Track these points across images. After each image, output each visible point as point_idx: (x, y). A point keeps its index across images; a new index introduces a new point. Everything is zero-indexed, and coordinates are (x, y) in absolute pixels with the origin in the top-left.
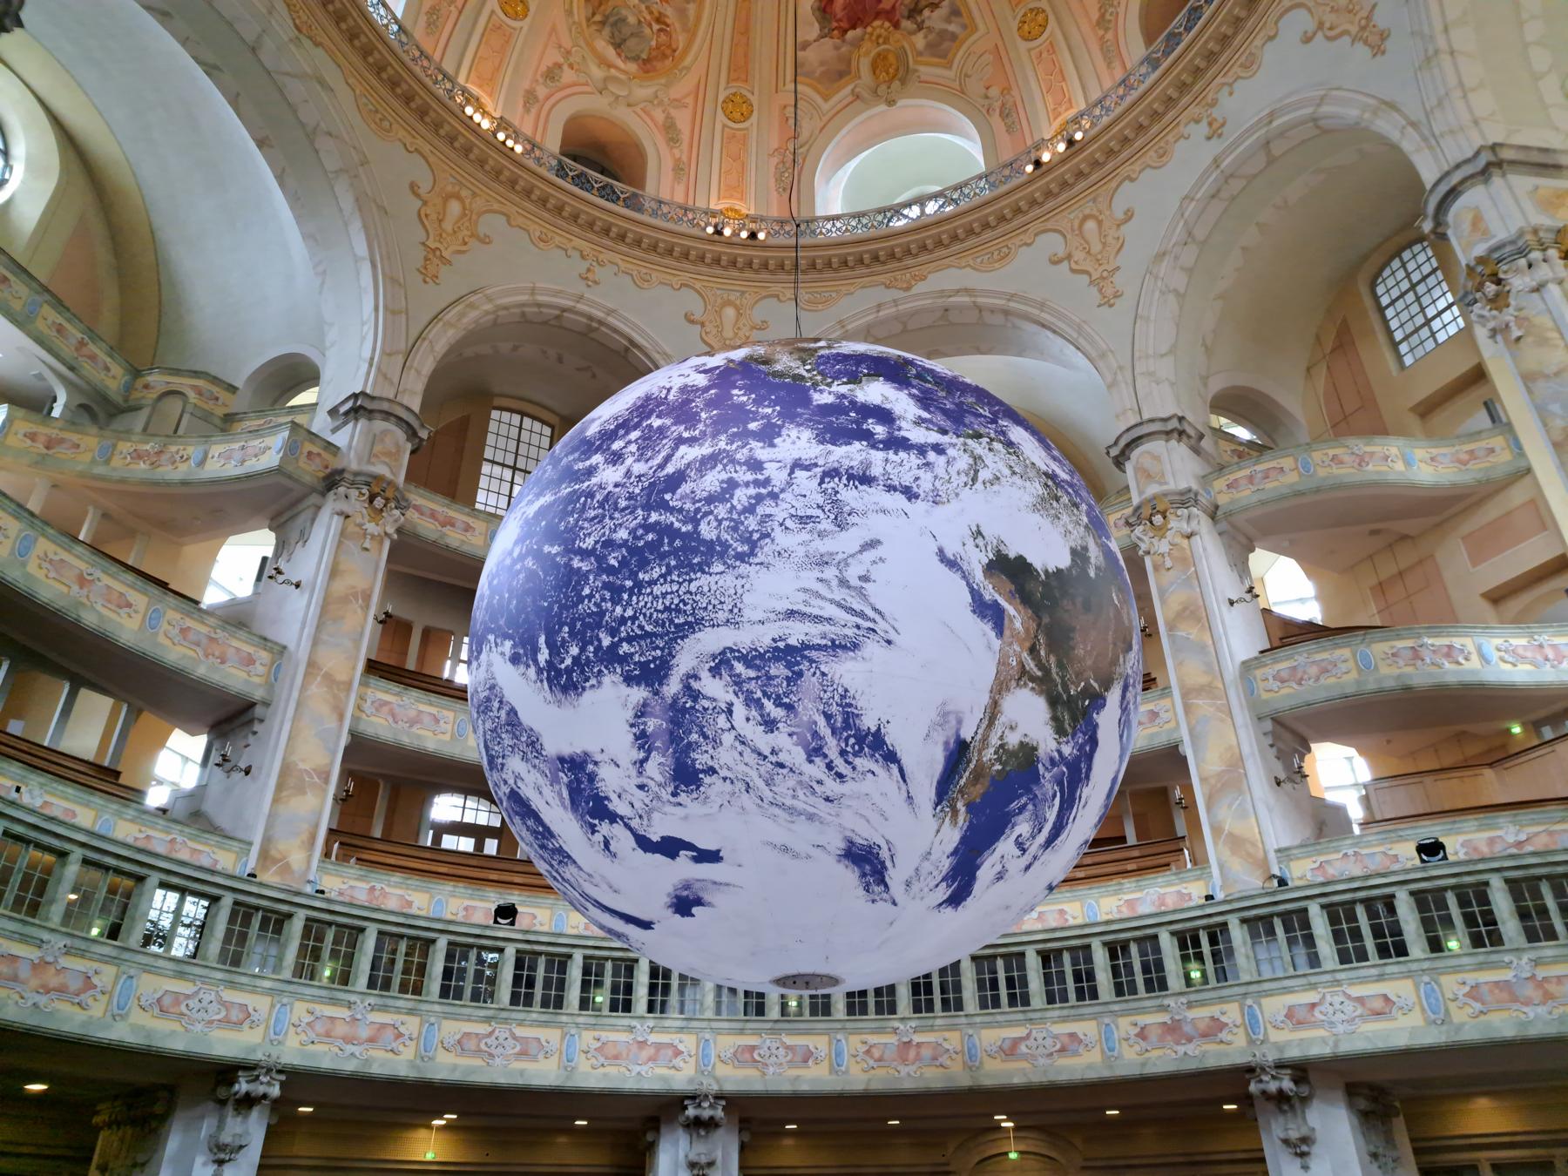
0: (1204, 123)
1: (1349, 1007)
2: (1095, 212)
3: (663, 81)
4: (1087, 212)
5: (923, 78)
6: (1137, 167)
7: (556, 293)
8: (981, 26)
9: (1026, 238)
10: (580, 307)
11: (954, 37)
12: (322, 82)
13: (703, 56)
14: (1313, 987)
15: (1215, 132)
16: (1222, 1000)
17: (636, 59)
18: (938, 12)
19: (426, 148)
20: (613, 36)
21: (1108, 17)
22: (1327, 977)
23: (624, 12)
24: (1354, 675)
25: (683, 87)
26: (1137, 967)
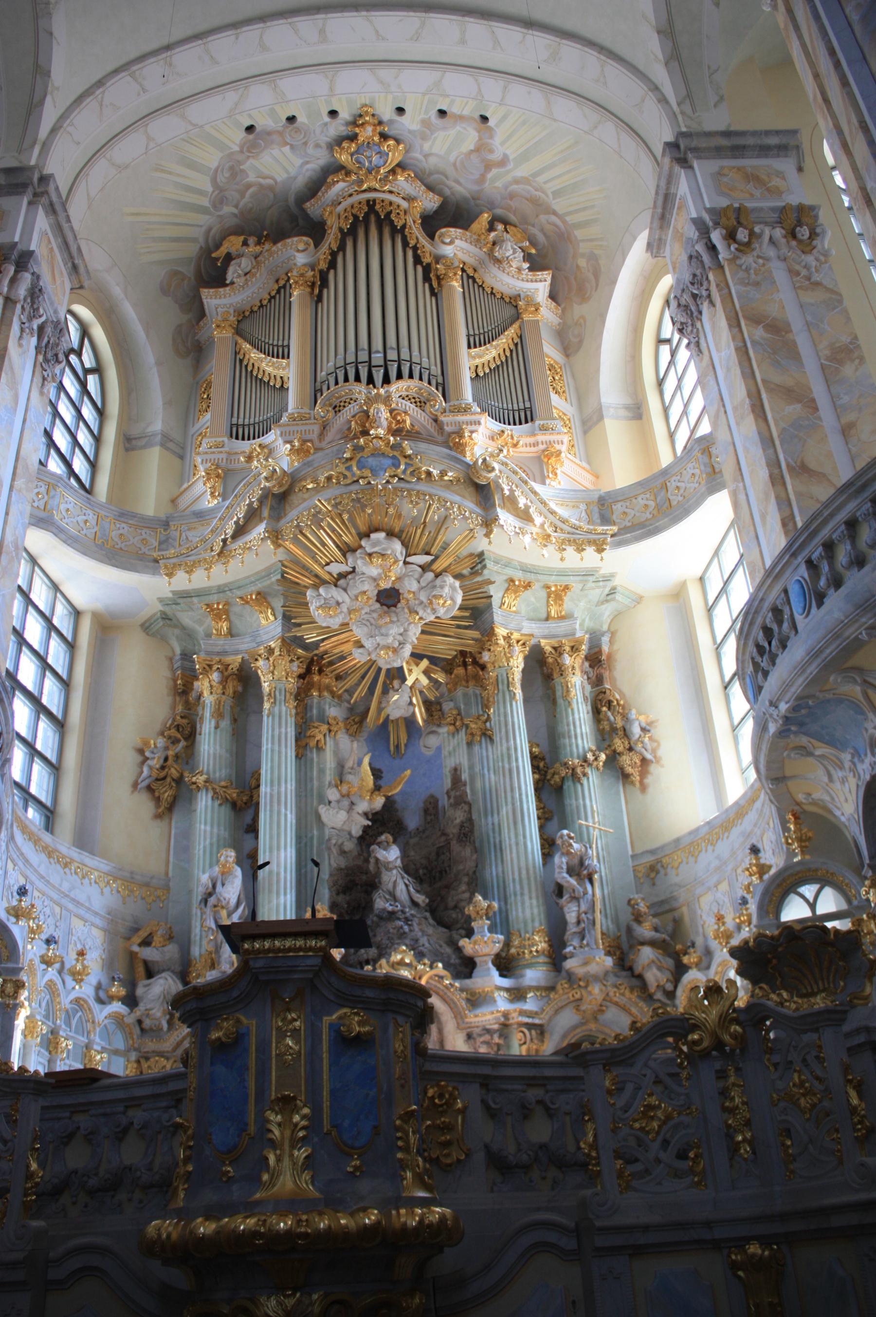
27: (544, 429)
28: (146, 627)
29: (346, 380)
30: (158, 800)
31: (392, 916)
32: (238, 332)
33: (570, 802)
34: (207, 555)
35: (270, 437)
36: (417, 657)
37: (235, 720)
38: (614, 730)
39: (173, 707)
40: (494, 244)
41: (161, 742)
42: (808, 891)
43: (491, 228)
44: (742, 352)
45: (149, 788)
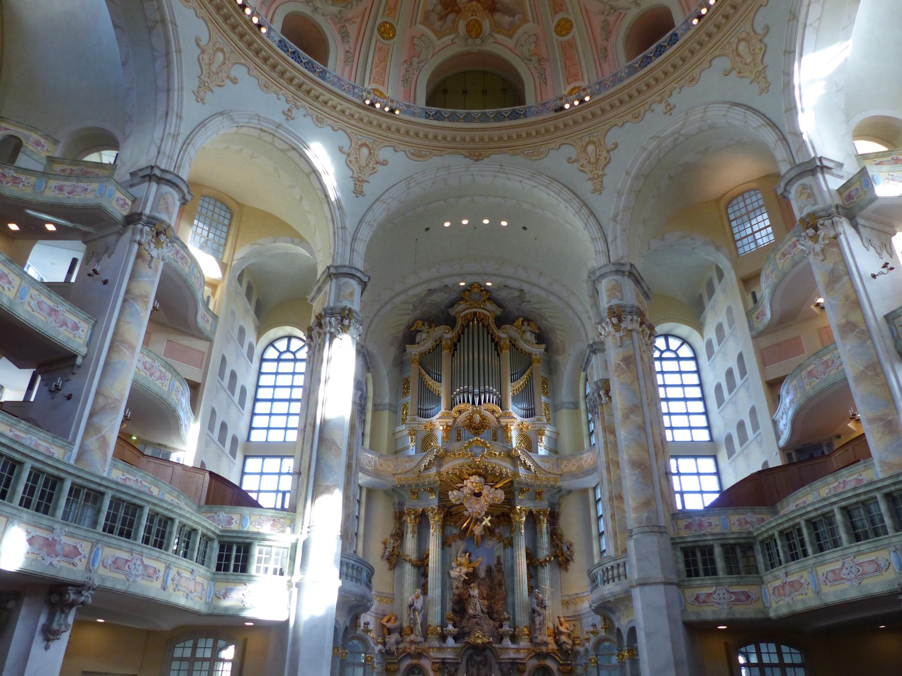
1: (141, 567)
2: (227, 55)
6: (255, 73)
9: (199, 10)
14: (131, 551)
15: (288, 115)
16: (85, 538)
22: (139, 549)
24: (166, 389)
26: (37, 493)
27: (538, 420)
28: (386, 492)
29: (464, 401)
30: (390, 563)
31: (474, 616)
32: (421, 364)
33: (540, 575)
34: (413, 475)
35: (434, 419)
36: (487, 515)
37: (419, 533)
38: (557, 545)
39: (395, 524)
40: (524, 332)
41: (392, 541)
42: (607, 644)
43: (523, 324)
44: (606, 443)
45: (388, 559)
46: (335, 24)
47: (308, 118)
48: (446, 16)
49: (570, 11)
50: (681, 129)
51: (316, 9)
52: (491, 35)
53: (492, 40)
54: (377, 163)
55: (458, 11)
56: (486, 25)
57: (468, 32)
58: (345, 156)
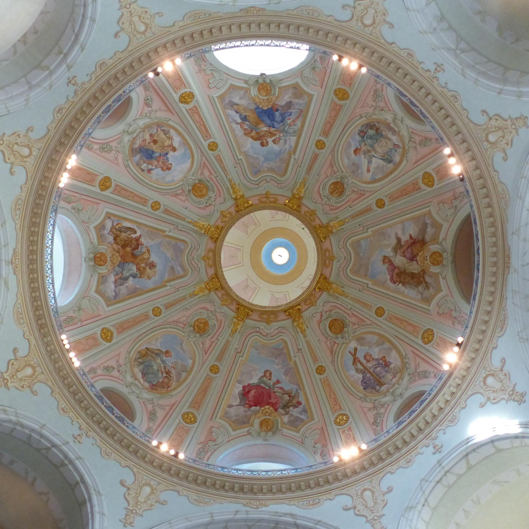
0: (431, 446)
2: (370, 487)
3: (158, 396)
4: (366, 487)
5: (284, 434)
6: (395, 467)
7: (55, 434)
8: (316, 419)
9: (329, 496)
10: (64, 448)
11: (302, 420)
12: (6, 283)
13: (182, 395)
15: (437, 450)
17: (149, 382)
18: (296, 410)
19: (33, 342)
20: (144, 369)
21: (378, 421)
23: (153, 363)
25: (166, 401)
46: (415, 381)
47: (448, 430)
48: (426, 283)
49: (416, 176)
50: (449, 49)
51: (401, 394)
52: (440, 244)
53: (444, 243)
54: (502, 370)
55: (423, 271)
56: (434, 248)
57: (438, 264)
58: (489, 402)
